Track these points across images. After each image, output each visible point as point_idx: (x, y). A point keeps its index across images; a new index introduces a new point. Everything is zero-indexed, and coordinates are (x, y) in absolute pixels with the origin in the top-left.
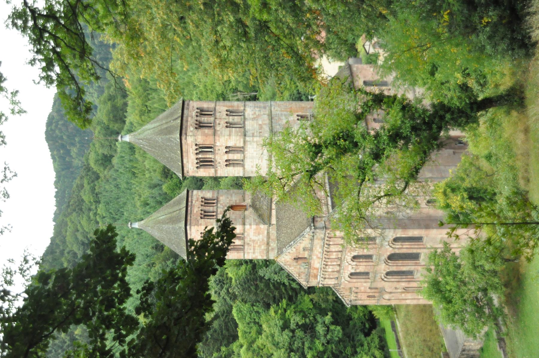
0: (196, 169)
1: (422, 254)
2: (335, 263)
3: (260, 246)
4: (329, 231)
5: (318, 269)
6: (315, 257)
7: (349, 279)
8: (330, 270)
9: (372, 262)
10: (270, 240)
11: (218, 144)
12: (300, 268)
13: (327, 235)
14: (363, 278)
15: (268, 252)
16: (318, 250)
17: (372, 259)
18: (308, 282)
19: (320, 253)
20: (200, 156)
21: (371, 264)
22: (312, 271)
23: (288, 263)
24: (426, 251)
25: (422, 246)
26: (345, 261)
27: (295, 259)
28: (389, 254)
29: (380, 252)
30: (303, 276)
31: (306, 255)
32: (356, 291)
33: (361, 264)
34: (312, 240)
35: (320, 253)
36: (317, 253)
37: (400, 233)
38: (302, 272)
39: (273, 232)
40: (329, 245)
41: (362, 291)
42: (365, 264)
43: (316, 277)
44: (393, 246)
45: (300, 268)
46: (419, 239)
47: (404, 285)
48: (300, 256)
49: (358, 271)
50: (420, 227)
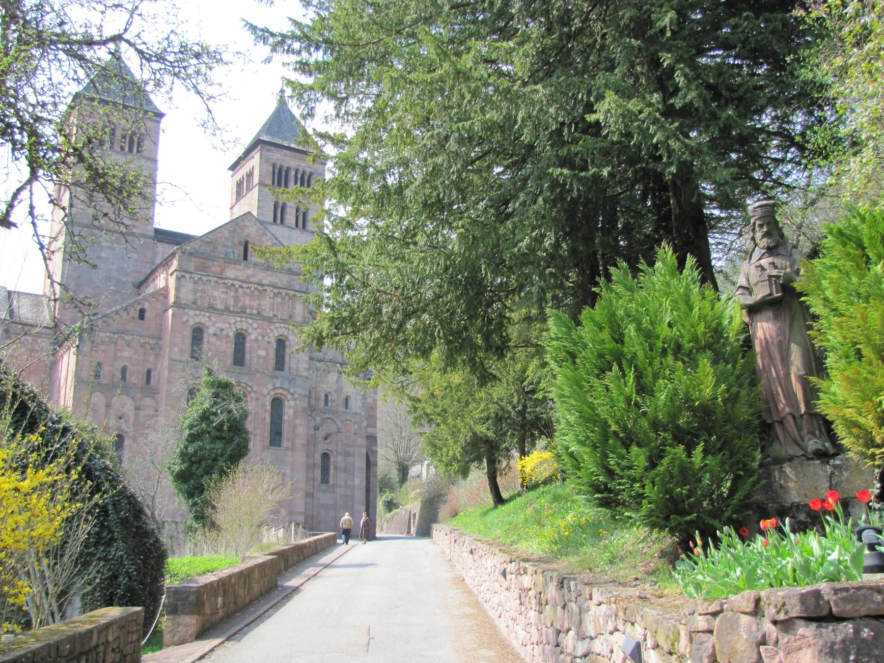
0: (273, 161)
5: (221, 273)
6: (250, 272)
8: (216, 294)
12: (224, 246)
18: (191, 254)
20: (293, 173)
22: (216, 264)
29: (258, 375)
36: (260, 277)
38: (215, 248)
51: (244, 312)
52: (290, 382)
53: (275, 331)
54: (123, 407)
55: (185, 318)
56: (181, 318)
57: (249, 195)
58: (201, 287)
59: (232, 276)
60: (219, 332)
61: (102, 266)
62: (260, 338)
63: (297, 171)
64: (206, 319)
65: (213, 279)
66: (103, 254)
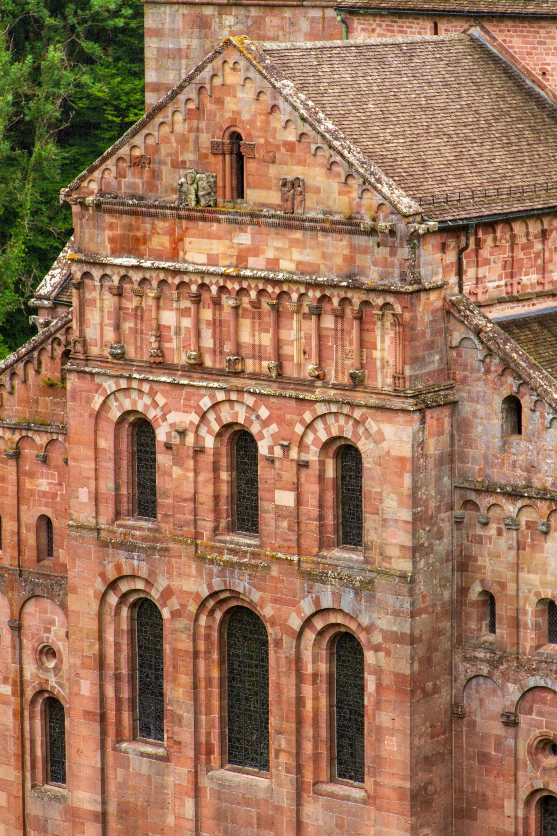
1: (262, 782)
2: (208, 342)
4: (398, 309)
6: (244, 239)
7: (115, 414)
8: (168, 318)
9: (216, 530)
10: (254, 12)
13: (380, 301)
14: (117, 488)
16: (289, 255)
17: (231, 529)
18: (98, 206)
19: (273, 265)
21: (207, 526)
23: (210, 106)
24: (284, 796)
25: (309, 777)
26: (221, 396)
27: (236, 137)
28: (267, 611)
29: (275, 571)
30: (134, 181)
31: (261, 196)
32: (28, 452)
33: (205, 476)
34: (350, 226)
35: (273, 265)
36: (270, 254)
37: (383, 665)
38: (155, 175)
39: (304, 25)
40: (317, 312)
41: (28, 484)
42: (206, 492)
43: (131, 244)
44: (310, 636)
45: (178, 165)
46: (348, 756)
47: (81, 692)
48: (250, 166)
49: (163, 459)
50: (422, 762)
52: (357, 592)
53: (319, 425)
54: (48, 630)
55: (98, 400)
56: (89, 401)
58: (130, 304)
60: (176, 440)
62: (278, 452)
64: (147, 400)
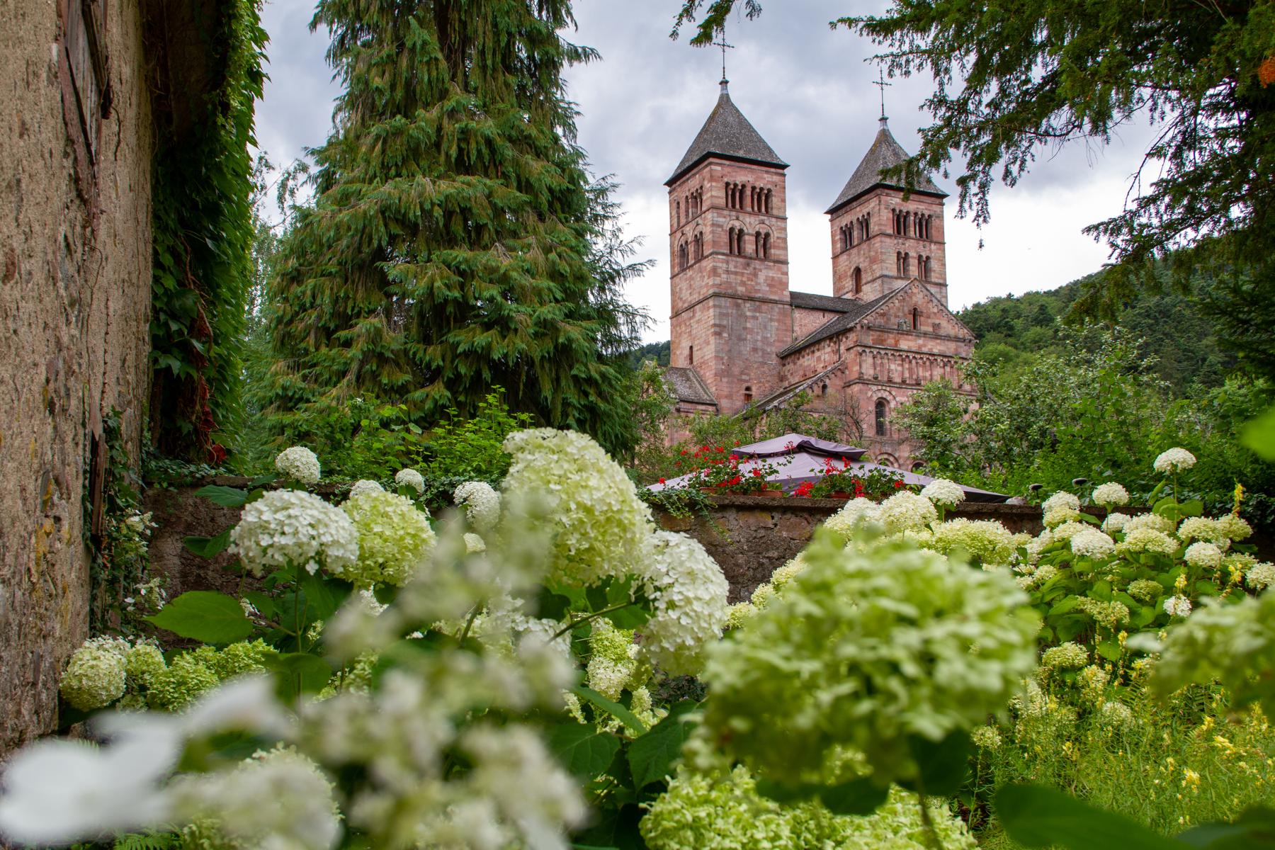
2: (907, 375)
3: (743, 284)
6: (921, 342)
8: (893, 367)
11: (933, 247)
12: (896, 316)
15: (733, 297)
16: (936, 347)
18: (869, 328)
30: (880, 321)
31: (926, 328)
34: (956, 339)
51: (919, 384)
55: (870, 393)
57: (864, 246)
59: (905, 348)
61: (749, 337)
63: (916, 214)
65: (890, 353)
66: (749, 325)
